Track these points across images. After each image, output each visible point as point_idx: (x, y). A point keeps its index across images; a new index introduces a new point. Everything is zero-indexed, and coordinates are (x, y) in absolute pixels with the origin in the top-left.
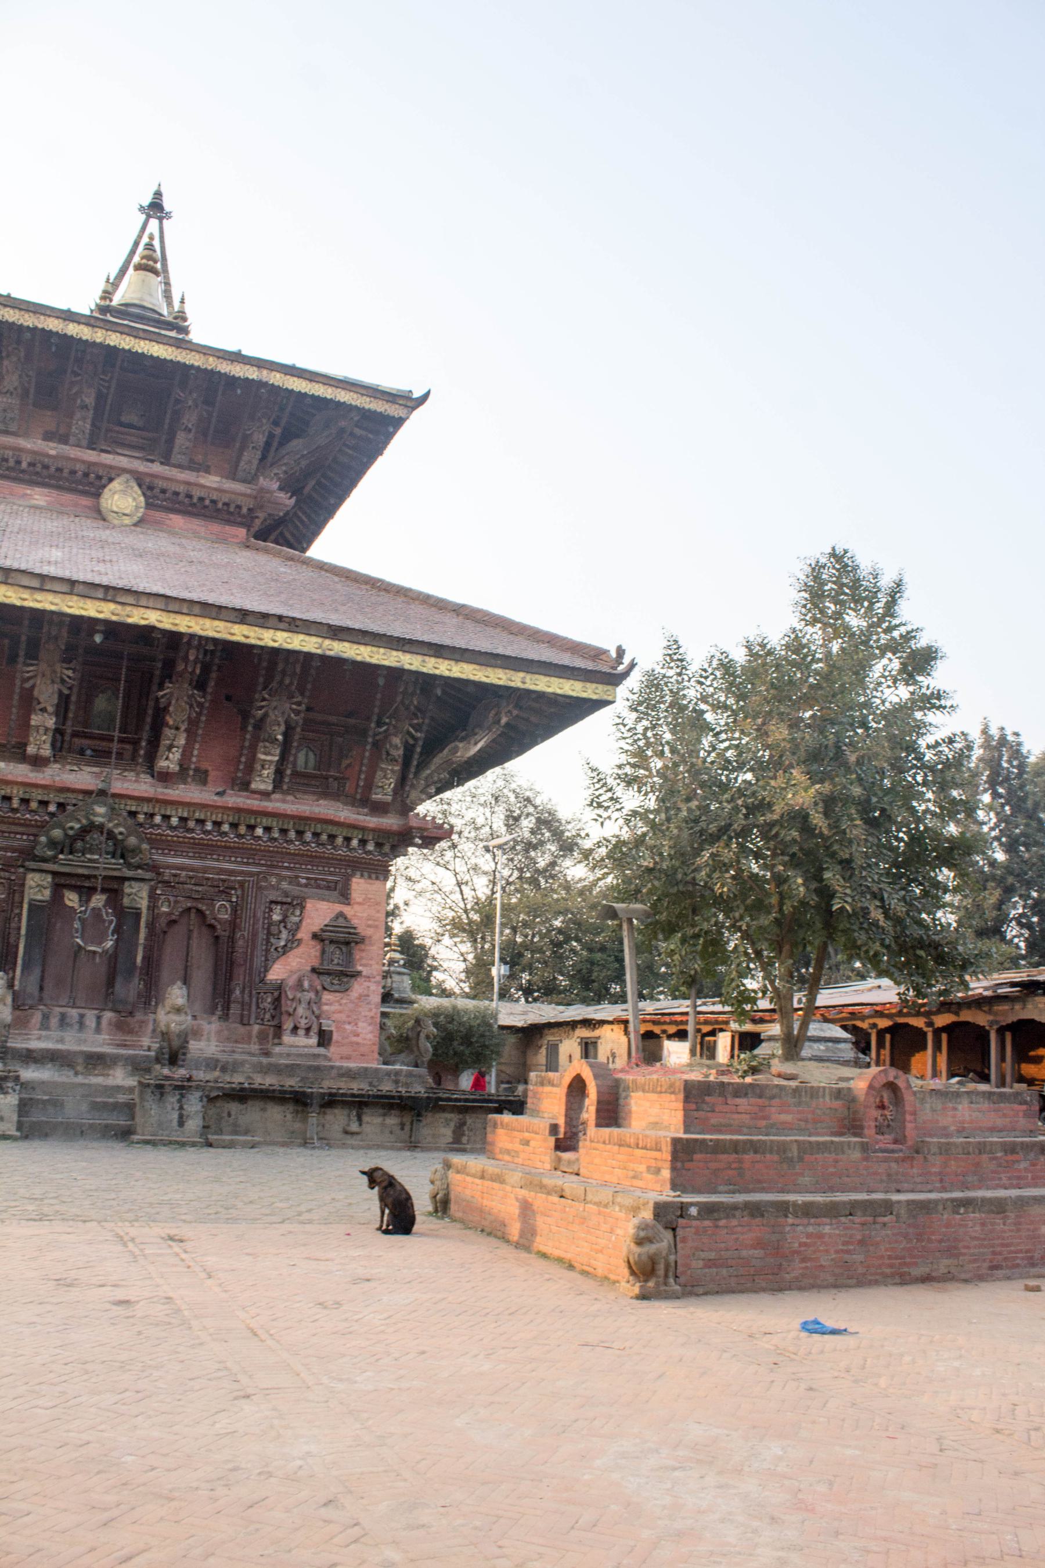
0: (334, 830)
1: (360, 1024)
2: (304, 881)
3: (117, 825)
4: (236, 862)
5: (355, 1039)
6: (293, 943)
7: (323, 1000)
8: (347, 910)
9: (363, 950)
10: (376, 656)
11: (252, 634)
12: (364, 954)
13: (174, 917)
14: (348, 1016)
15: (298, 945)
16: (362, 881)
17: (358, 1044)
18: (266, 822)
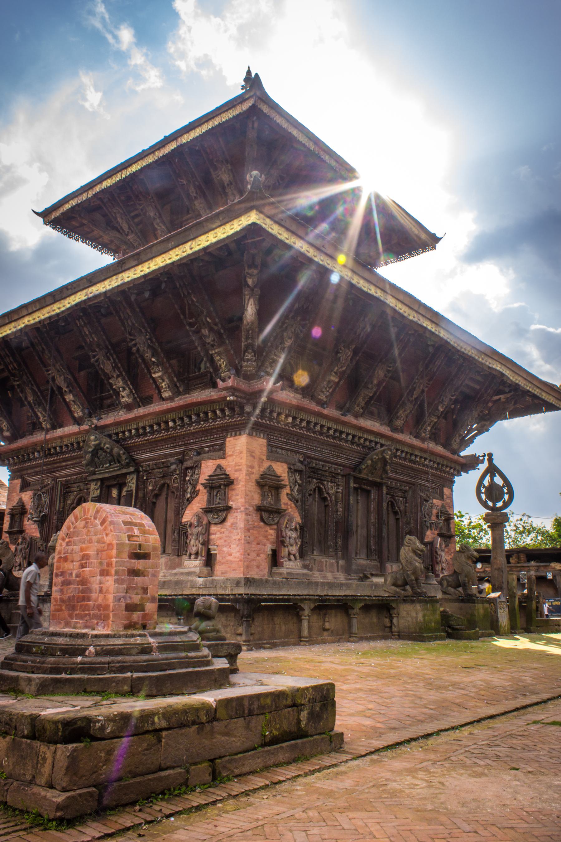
0: (203, 408)
1: (232, 546)
2: (207, 449)
3: (105, 444)
4: (168, 448)
5: (229, 558)
6: (195, 493)
7: (211, 532)
8: (222, 462)
9: (233, 490)
10: (113, 283)
11: (61, 306)
12: (233, 492)
13: (156, 492)
14: (225, 541)
15: (197, 495)
16: (232, 438)
17: (231, 561)
18: (170, 416)
